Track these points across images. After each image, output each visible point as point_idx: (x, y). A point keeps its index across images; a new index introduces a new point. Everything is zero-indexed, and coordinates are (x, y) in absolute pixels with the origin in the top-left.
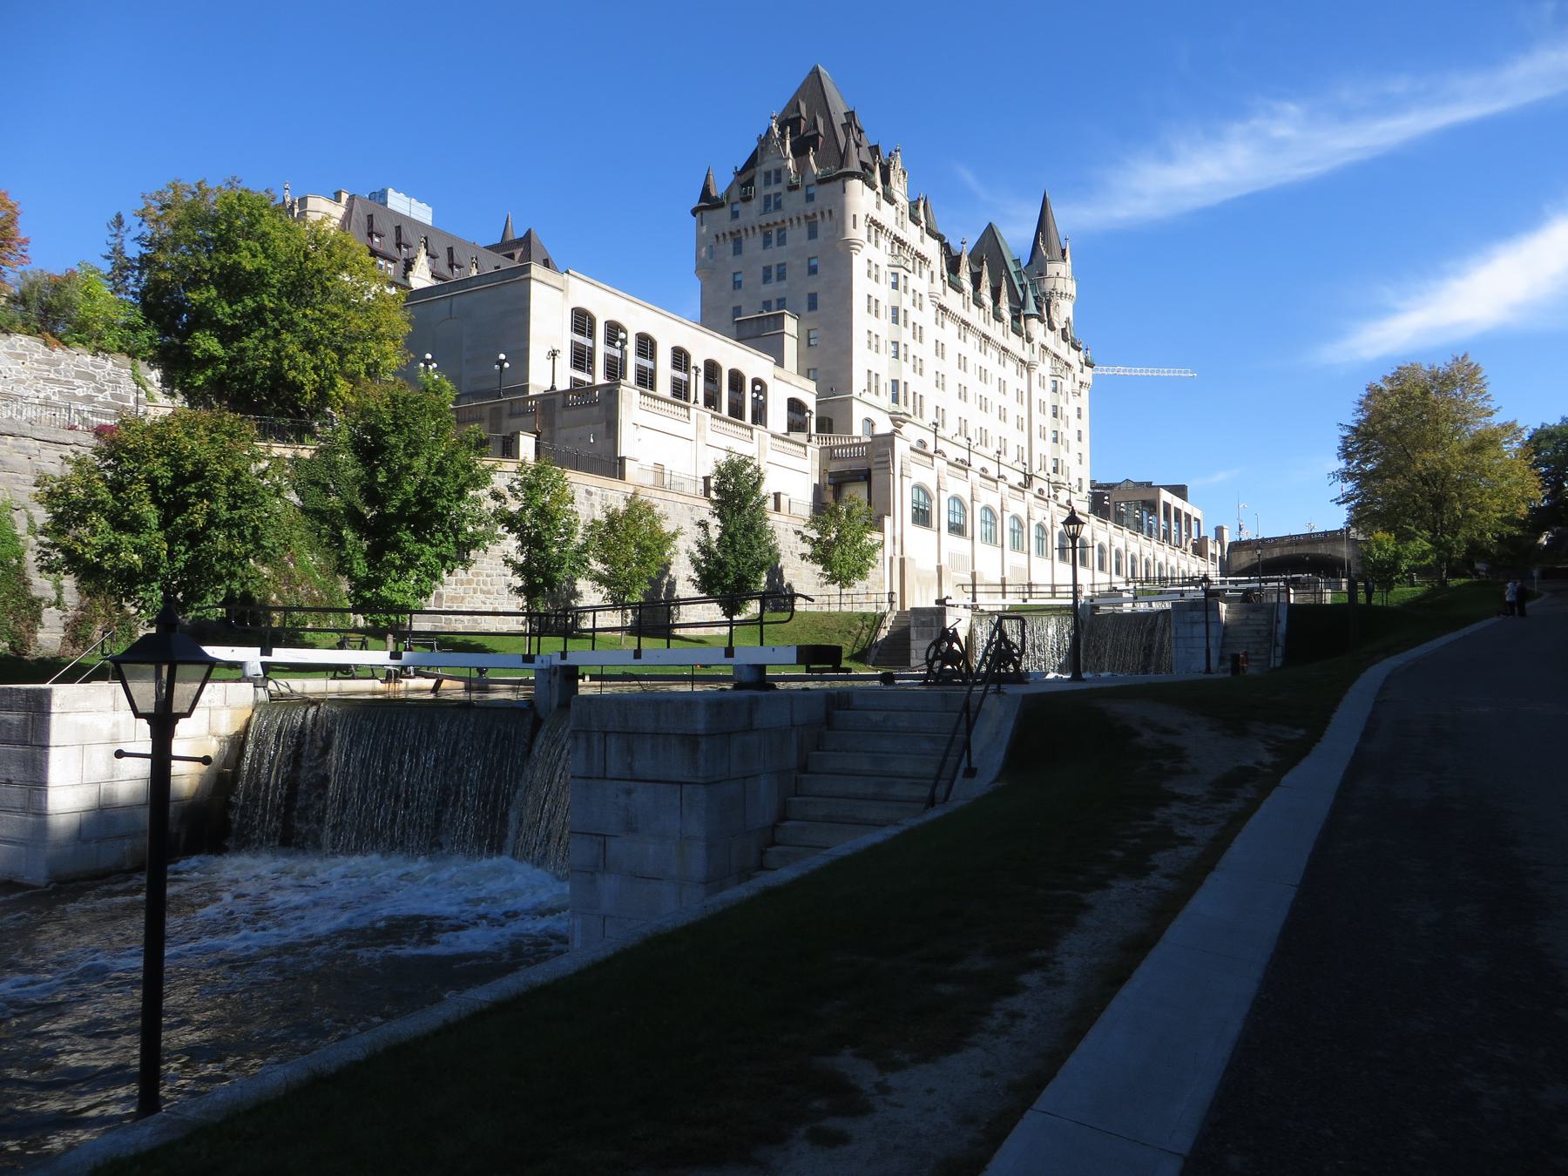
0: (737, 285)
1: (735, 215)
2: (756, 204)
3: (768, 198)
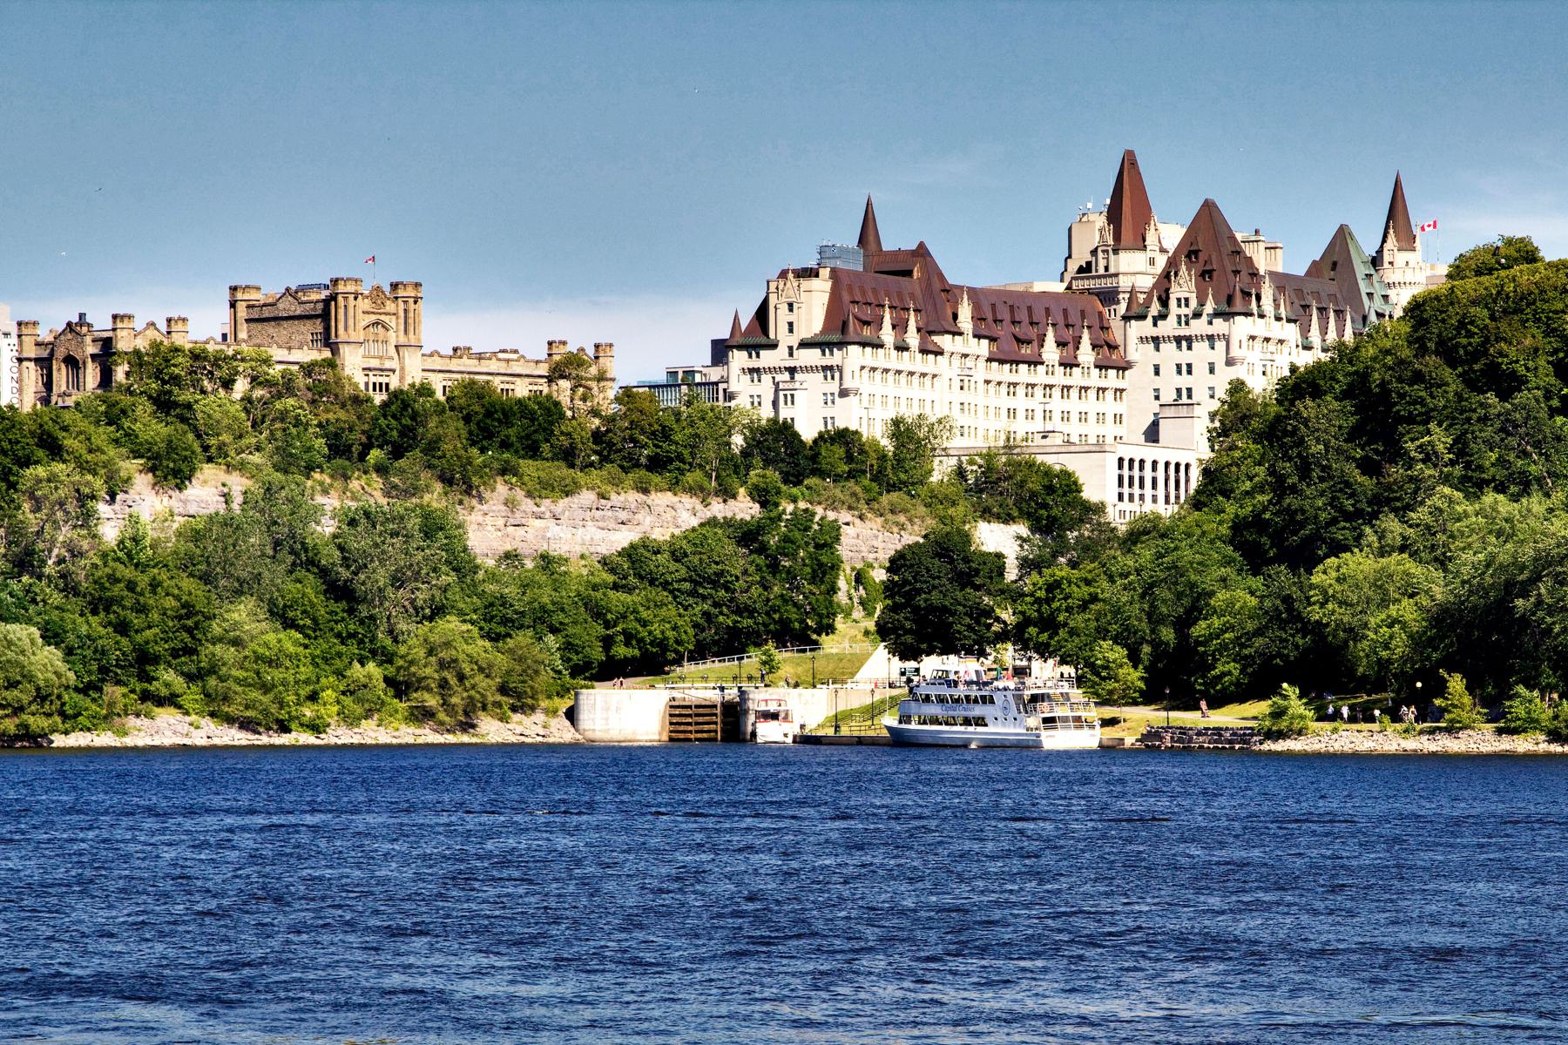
0: (1157, 373)
1: (1155, 325)
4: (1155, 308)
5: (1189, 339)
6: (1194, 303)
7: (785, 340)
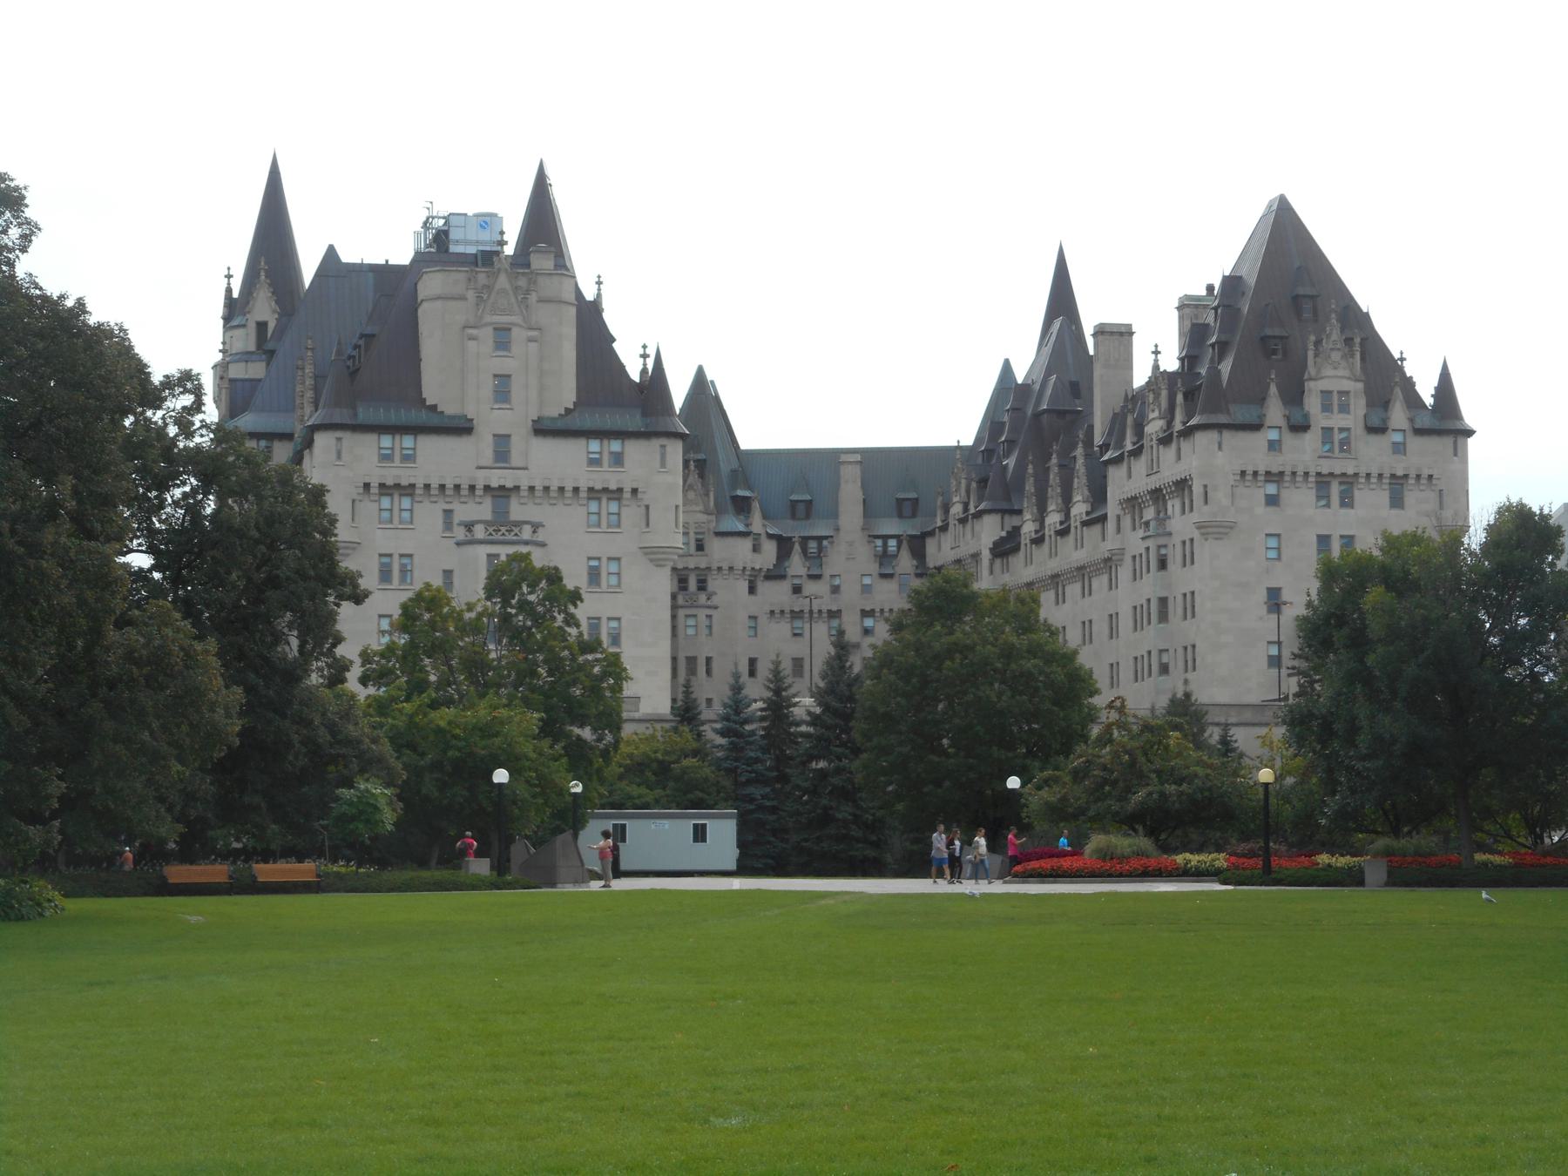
1: (1274, 446)
2: (1311, 440)
3: (1327, 431)
4: (1275, 411)
5: (1349, 482)
6: (1359, 406)
7: (491, 420)
